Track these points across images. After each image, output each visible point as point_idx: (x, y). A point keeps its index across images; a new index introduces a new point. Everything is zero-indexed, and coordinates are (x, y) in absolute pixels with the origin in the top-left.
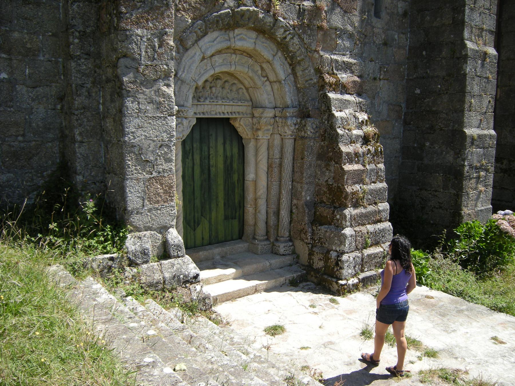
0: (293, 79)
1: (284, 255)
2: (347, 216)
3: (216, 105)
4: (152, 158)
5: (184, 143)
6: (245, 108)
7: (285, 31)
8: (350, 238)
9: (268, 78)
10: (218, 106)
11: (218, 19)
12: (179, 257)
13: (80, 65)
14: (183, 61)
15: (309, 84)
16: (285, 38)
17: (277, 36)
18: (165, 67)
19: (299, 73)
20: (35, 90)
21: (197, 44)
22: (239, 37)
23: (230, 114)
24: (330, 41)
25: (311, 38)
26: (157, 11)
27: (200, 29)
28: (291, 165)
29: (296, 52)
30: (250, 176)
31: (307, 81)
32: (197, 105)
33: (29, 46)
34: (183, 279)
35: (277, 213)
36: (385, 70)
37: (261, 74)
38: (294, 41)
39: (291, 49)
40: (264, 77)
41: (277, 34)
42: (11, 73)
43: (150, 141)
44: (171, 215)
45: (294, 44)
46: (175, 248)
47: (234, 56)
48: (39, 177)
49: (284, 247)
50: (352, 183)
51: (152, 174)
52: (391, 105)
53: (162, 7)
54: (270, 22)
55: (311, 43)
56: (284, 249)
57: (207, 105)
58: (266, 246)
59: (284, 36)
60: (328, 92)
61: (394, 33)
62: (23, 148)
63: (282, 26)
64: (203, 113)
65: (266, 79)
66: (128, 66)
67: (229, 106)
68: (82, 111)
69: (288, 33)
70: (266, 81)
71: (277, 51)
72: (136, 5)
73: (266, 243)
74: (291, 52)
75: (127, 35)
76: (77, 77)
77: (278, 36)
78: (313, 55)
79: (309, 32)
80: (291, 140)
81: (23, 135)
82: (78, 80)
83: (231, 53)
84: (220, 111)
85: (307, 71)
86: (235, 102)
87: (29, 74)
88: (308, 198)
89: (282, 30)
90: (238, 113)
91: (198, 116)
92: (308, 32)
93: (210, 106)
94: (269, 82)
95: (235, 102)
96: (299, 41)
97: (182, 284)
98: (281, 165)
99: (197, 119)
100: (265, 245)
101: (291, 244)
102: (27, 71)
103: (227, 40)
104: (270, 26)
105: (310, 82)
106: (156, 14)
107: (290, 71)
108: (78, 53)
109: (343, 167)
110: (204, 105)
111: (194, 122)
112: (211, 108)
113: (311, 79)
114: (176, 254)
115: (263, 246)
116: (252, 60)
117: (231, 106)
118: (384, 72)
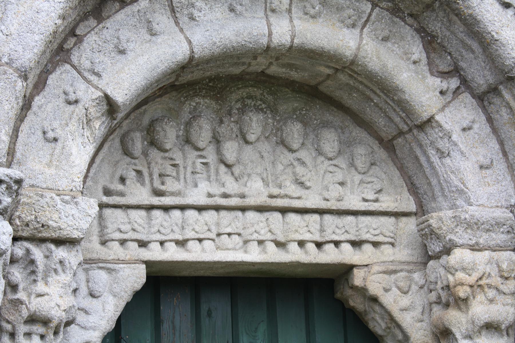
10: (251, 215)
32: (150, 208)
37: (430, 63)
40: (444, 75)
57: (200, 209)
64: (181, 243)
65: (454, 83)
67: (307, 217)
90: (356, 244)
93: (210, 216)
110: (183, 208)
112: (218, 224)
116: (375, 5)
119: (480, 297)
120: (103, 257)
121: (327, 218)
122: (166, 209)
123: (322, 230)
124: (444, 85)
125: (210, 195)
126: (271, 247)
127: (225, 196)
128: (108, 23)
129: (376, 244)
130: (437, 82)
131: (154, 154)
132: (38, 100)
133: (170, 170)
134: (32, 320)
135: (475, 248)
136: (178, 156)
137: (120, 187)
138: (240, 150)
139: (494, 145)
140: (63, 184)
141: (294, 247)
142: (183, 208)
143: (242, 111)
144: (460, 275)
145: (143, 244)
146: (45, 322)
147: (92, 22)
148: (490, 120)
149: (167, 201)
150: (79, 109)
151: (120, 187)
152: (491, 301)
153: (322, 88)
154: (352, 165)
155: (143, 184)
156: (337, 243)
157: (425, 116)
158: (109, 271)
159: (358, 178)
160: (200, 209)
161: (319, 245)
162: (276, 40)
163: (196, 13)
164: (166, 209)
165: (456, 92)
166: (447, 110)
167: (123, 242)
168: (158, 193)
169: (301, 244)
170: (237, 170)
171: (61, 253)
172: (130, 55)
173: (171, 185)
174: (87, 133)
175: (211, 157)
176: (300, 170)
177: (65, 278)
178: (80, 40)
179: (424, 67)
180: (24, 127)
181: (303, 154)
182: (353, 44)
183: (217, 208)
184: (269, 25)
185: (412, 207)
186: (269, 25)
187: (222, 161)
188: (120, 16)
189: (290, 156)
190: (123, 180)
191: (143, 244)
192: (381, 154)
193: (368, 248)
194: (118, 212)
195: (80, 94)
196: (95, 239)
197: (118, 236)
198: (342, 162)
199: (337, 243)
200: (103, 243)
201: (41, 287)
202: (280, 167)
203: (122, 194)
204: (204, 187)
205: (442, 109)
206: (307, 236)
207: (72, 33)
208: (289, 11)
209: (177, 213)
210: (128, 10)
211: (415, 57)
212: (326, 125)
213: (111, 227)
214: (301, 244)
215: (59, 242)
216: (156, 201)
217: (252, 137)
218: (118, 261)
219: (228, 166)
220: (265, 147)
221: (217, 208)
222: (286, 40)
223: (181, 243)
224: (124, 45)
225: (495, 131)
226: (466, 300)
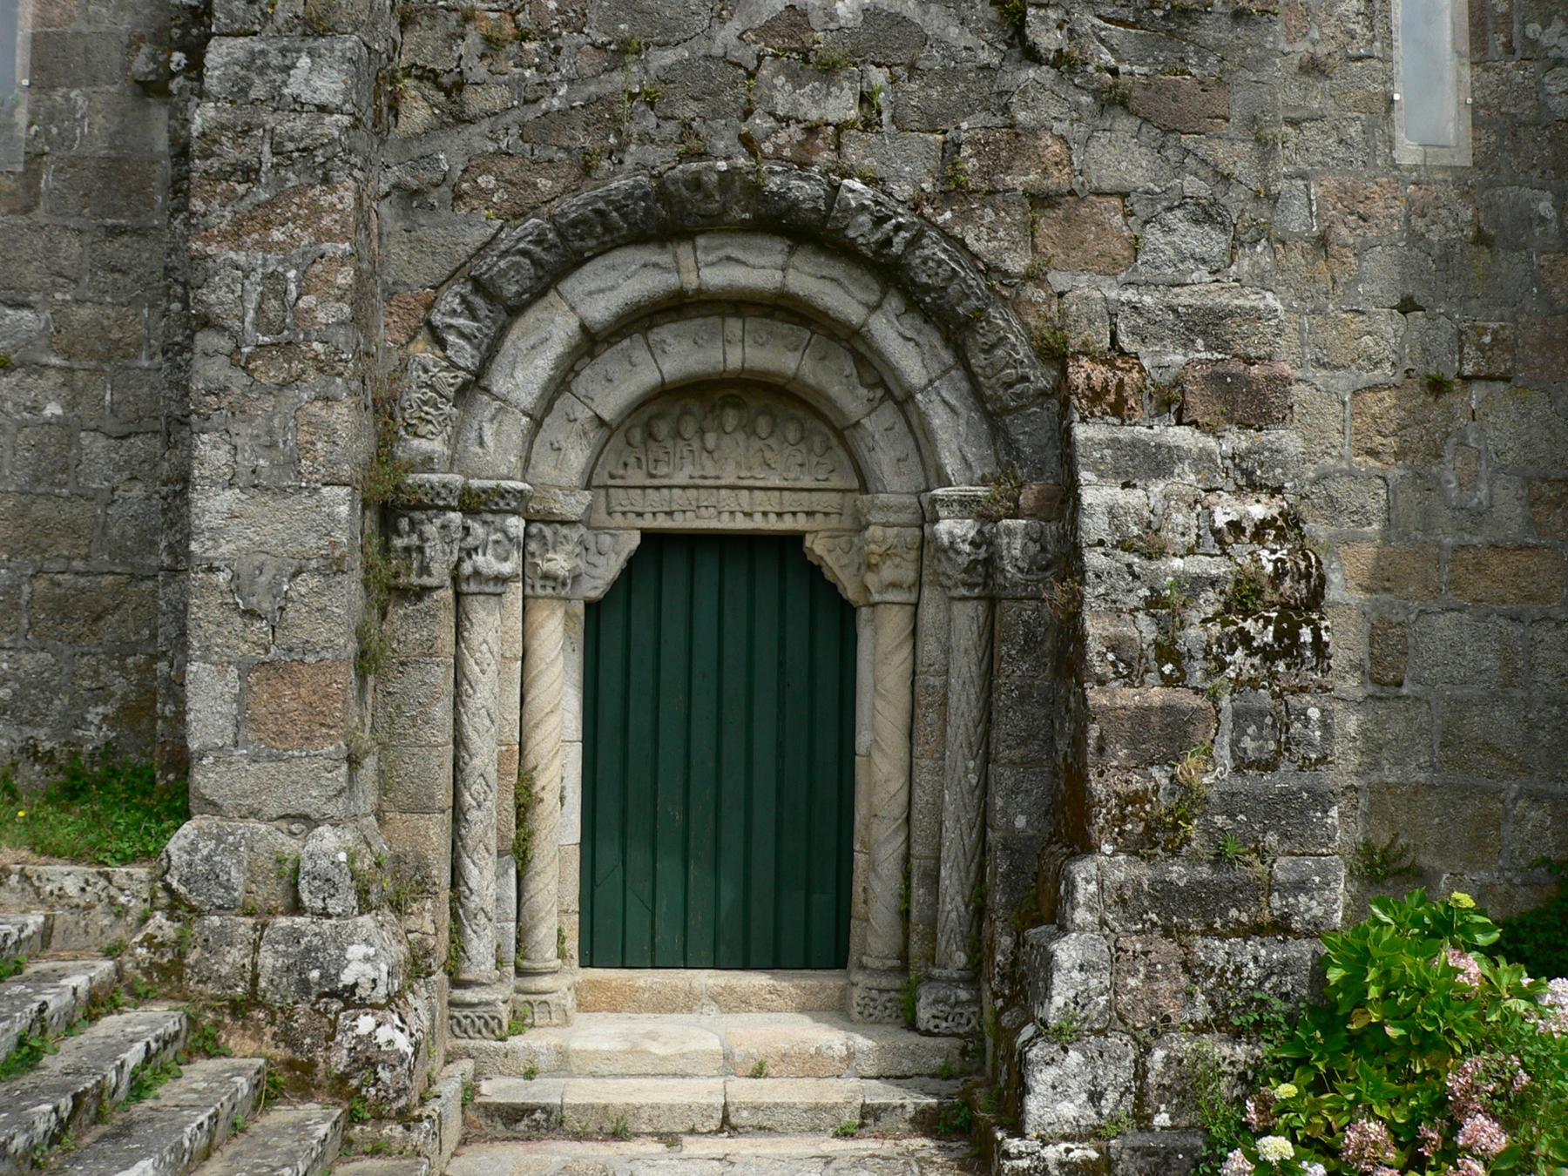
0: (964, 386)
1: (928, 1033)
2: (1080, 884)
3: (718, 488)
4: (266, 605)
5: (592, 607)
6: (834, 499)
7: (879, 221)
8: (1075, 974)
9: (888, 391)
10: (723, 492)
11: (601, 205)
12: (329, 916)
13: (179, 367)
14: (508, 343)
15: (1019, 396)
16: (888, 242)
17: (854, 239)
18: (317, 346)
19: (978, 361)
20: (126, 443)
21: (560, 294)
22: (712, 258)
23: (772, 517)
24: (1098, 238)
25: (1001, 234)
26: (296, 200)
27: (538, 242)
28: (973, 697)
29: (944, 288)
30: (863, 740)
31: (1011, 385)
32: (644, 488)
33: (116, 334)
34: (319, 984)
35: (933, 878)
36: (1487, 339)
37: (860, 376)
38: (927, 252)
39: (924, 279)
40: (871, 387)
41: (851, 234)
42: (69, 405)
43: (263, 557)
44: (323, 782)
45: (931, 264)
46: (317, 883)
47: (734, 326)
48: (114, 669)
49: (936, 1002)
50: (1130, 757)
51: (267, 651)
52: (1545, 480)
53: (312, 186)
54: (815, 199)
55: (998, 252)
56: (934, 1012)
57: (684, 488)
58: (885, 997)
59: (878, 236)
60: (1083, 420)
61: (1527, 192)
62: (83, 591)
63: (863, 208)
64: (670, 514)
65: (879, 393)
66: (210, 351)
68: (178, 488)
69: (888, 226)
70: (882, 400)
71: (884, 294)
72: (234, 191)
73: (885, 983)
74: (927, 289)
75: (206, 270)
76: (170, 398)
77: (860, 240)
78: (1018, 294)
79: (989, 214)
80: (971, 605)
81: (86, 558)
82: (174, 406)
83: (723, 316)
84: (734, 507)
85: (1000, 352)
86: (792, 475)
87: (112, 402)
88: (1021, 822)
89: (864, 218)
90: (809, 514)
91: (648, 523)
92: (982, 218)
93: (692, 493)
94: (896, 402)
95: (792, 475)
96: (945, 251)
97: (313, 998)
98: (944, 703)
99: (647, 535)
100: (881, 991)
101: (963, 995)
102: (108, 397)
103: (666, 269)
104: (816, 210)
105: (1019, 387)
106: (294, 208)
107: (947, 357)
108: (179, 339)
109: (1090, 694)
110: (670, 487)
111: (634, 540)
113: (1025, 379)
114: (320, 904)
115: (874, 993)
116: (813, 333)
117: (777, 494)
118: (1481, 348)
119: (888, 563)
120: (607, 524)
121: (786, 494)
122: (658, 488)
123: (781, 503)
124: (871, 395)
125: (691, 477)
126: (740, 516)
127: (705, 478)
128: (599, 360)
129: (826, 514)
130: (863, 392)
131: (652, 445)
132: (547, 420)
133: (662, 456)
134: (546, 576)
135: (886, 525)
136: (669, 444)
137: (621, 472)
138: (718, 439)
139: (910, 442)
140: (564, 482)
141: (758, 517)
142: (670, 487)
143: (722, 408)
144: (873, 547)
145: (640, 515)
146: (555, 579)
147: (587, 360)
148: (908, 423)
149: (656, 482)
150: (577, 425)
151: (621, 472)
152: (897, 566)
153: (788, 387)
154: (810, 450)
155: (640, 467)
156: (794, 514)
157: (854, 420)
158: (612, 535)
159: (815, 460)
160: (684, 488)
161: (779, 515)
162: (730, 366)
163: (667, 348)
164: (658, 488)
165: (882, 400)
166: (873, 416)
167: (624, 513)
168: (652, 476)
169: (765, 514)
170: (716, 455)
171: (564, 531)
172: (616, 383)
173: (663, 469)
174: (584, 442)
175: (696, 446)
176: (768, 454)
177: (569, 547)
178: (577, 374)
179: (854, 379)
180: (538, 441)
181: (771, 441)
182: (793, 366)
183: (697, 487)
184: (725, 353)
185: (856, 484)
186: (725, 353)
187: (704, 448)
188: (607, 354)
189: (761, 444)
190: (626, 465)
191: (640, 515)
192: (834, 442)
193: (819, 517)
194: (621, 491)
195: (578, 415)
196: (603, 510)
197: (619, 508)
198: (802, 447)
199: (794, 514)
200: (610, 514)
201: (550, 555)
202: (752, 452)
203: (622, 477)
204: (688, 469)
205: (868, 415)
206: (769, 508)
207: (572, 369)
208: (743, 341)
209: (665, 492)
210: (615, 348)
211: (847, 373)
212: (792, 418)
213: (614, 503)
214: (765, 514)
215: (563, 523)
216: (648, 482)
217: (729, 429)
218: (619, 528)
219: (710, 452)
220: (741, 437)
221: (697, 487)
222: (738, 365)
223: (670, 514)
224: (610, 375)
225: (912, 431)
226: (876, 565)
